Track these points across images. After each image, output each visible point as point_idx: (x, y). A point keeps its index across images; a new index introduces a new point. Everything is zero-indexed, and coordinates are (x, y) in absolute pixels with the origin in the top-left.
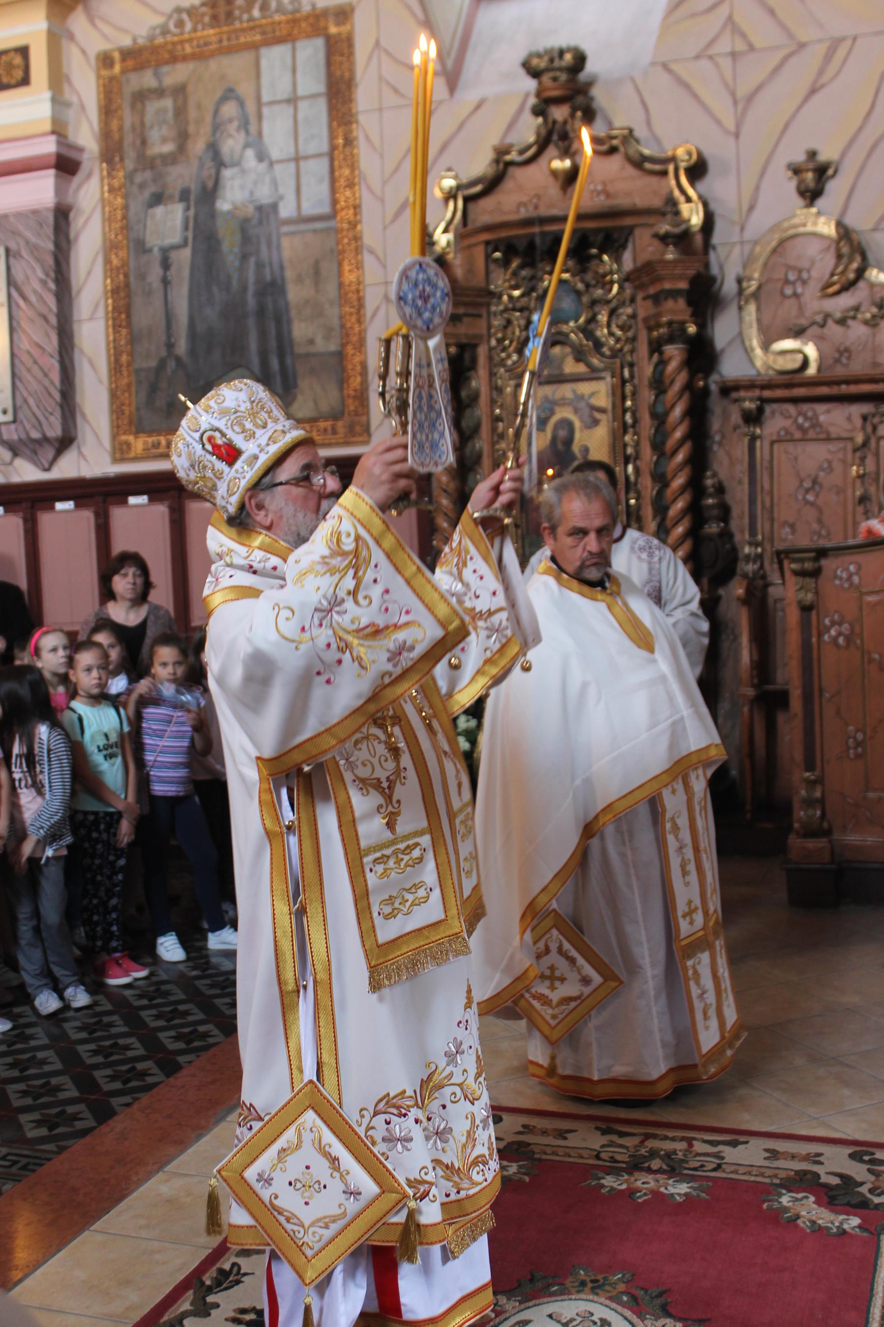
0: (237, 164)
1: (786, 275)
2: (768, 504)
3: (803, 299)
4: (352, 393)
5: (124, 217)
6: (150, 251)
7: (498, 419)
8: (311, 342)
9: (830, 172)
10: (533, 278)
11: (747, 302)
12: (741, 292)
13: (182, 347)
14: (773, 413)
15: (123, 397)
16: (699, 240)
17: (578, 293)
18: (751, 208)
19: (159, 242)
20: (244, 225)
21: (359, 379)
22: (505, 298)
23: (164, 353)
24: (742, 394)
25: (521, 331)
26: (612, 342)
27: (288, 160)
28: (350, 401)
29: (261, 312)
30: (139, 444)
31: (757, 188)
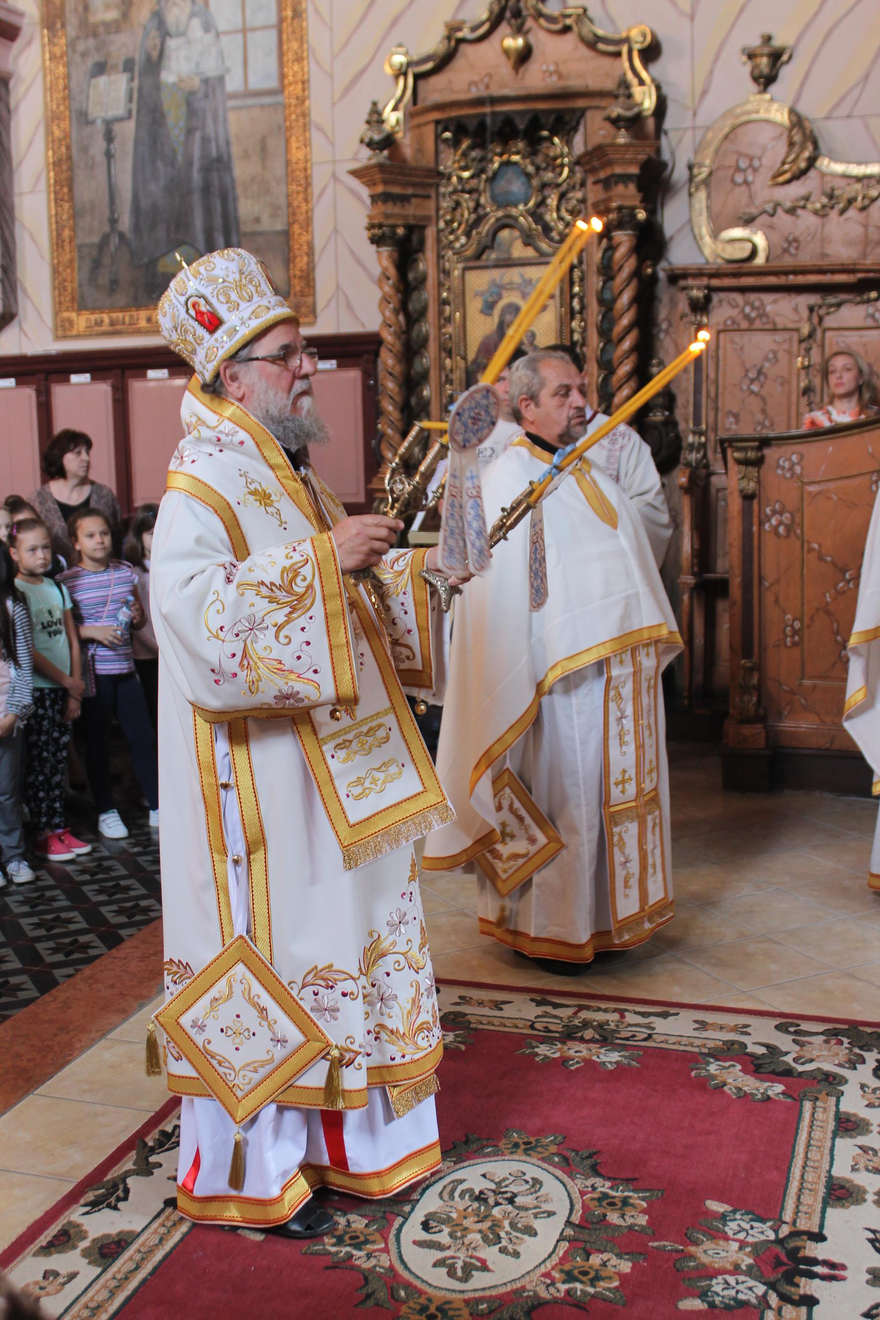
0: (183, 34)
1: (737, 161)
2: (712, 394)
3: (753, 187)
4: (298, 273)
5: (66, 87)
6: (93, 122)
7: (445, 302)
8: (257, 220)
9: (785, 58)
10: (482, 159)
11: (697, 189)
12: (691, 178)
13: (125, 223)
14: (720, 301)
16: (651, 124)
17: (528, 176)
18: (705, 93)
19: (102, 114)
20: (190, 101)
21: (305, 259)
22: (454, 179)
23: (107, 228)
24: (690, 282)
25: (470, 214)
26: (561, 226)
27: (235, 32)
28: (296, 282)
29: (206, 189)
30: (82, 321)
31: (711, 72)
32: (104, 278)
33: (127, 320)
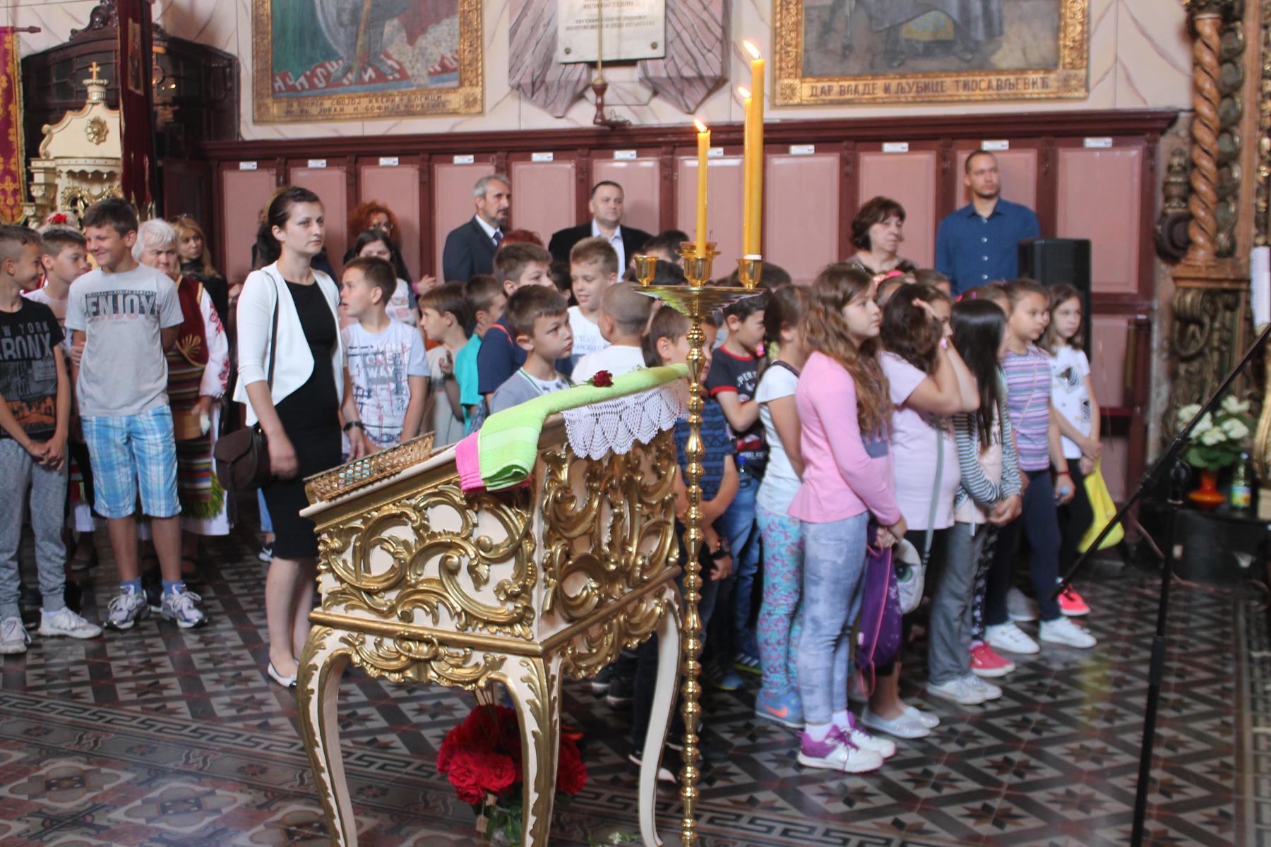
4: (1070, 44)
15: (788, 38)
21: (1079, 28)
30: (805, 90)
32: (835, 43)
33: (861, 88)
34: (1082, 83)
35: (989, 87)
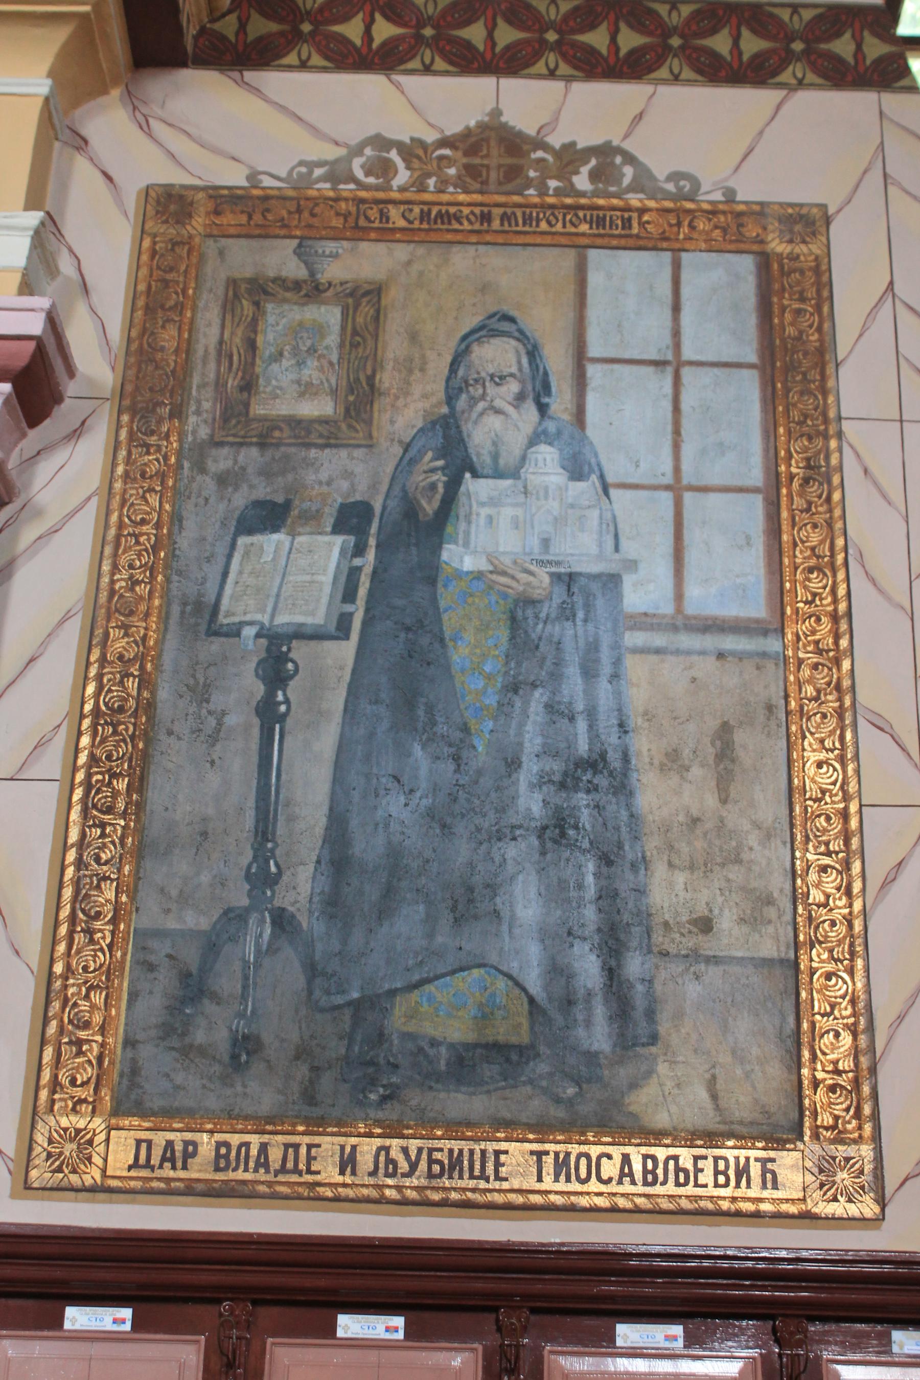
6: (235, 632)
8: (705, 925)
15: (84, 1005)
33: (275, 1155)
34: (867, 1178)
35: (626, 1173)
